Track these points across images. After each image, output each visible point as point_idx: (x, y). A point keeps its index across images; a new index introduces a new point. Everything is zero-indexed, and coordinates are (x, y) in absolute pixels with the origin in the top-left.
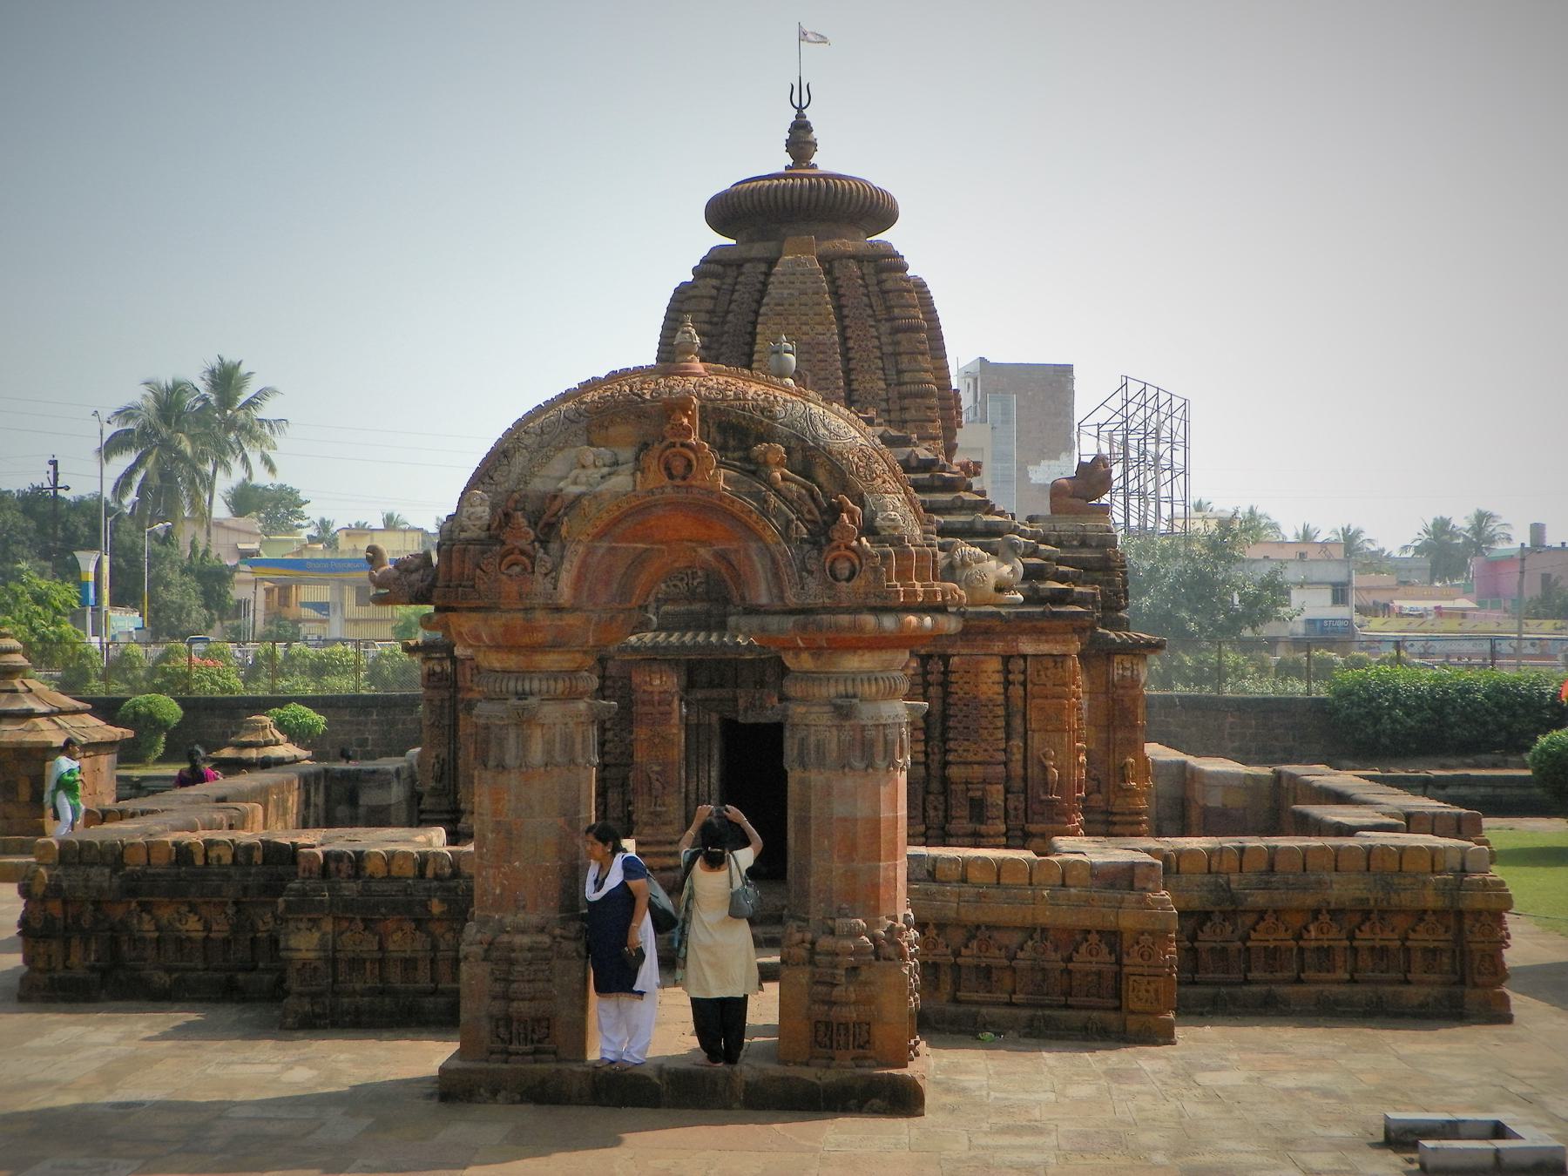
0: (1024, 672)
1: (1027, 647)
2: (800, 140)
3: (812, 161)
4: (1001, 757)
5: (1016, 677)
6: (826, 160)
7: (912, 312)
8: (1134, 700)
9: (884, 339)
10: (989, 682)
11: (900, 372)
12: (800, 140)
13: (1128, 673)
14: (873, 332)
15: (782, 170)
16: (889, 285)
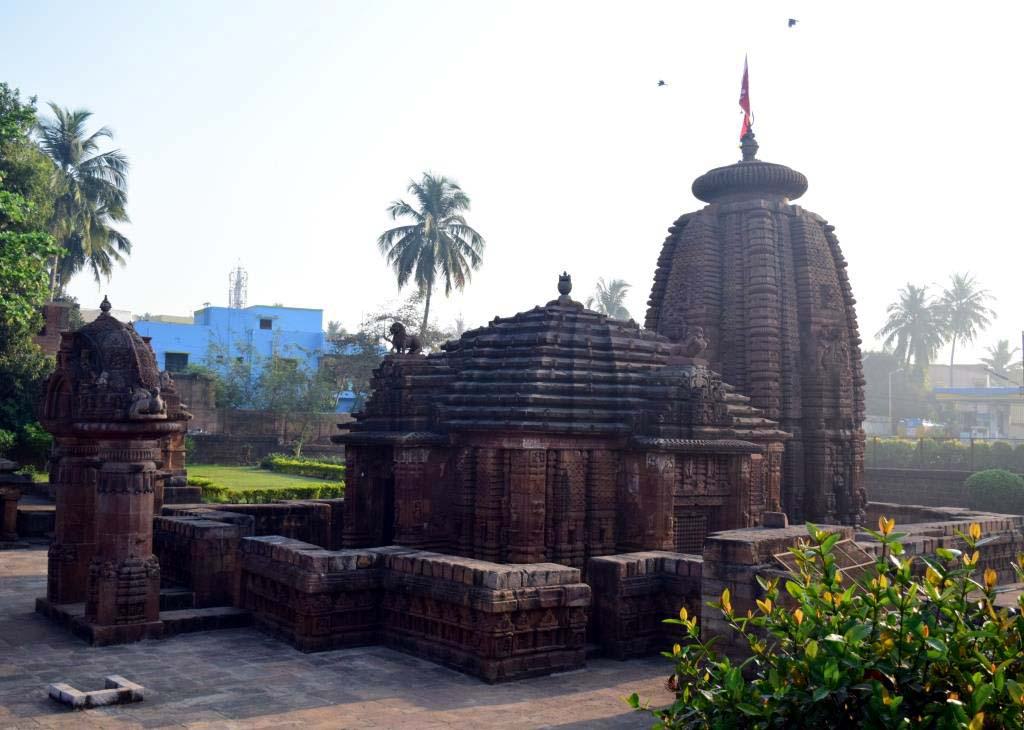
0: (510, 458)
1: (506, 445)
2: (748, 142)
3: (757, 157)
4: (495, 505)
5: (507, 461)
6: (761, 156)
7: (759, 241)
8: (656, 480)
9: (746, 260)
10: (489, 465)
11: (750, 278)
12: (748, 142)
13: (653, 463)
14: (739, 256)
15: (735, 162)
16: (751, 227)
